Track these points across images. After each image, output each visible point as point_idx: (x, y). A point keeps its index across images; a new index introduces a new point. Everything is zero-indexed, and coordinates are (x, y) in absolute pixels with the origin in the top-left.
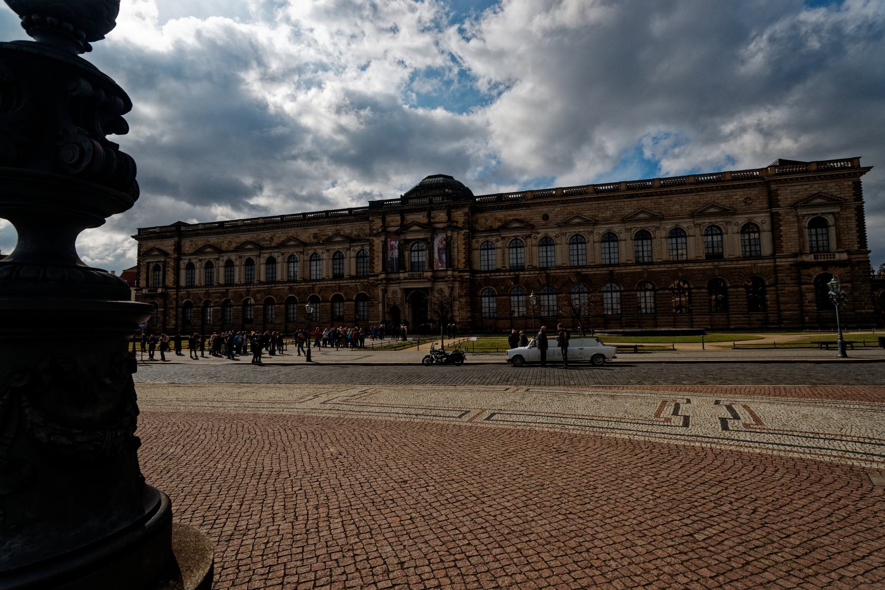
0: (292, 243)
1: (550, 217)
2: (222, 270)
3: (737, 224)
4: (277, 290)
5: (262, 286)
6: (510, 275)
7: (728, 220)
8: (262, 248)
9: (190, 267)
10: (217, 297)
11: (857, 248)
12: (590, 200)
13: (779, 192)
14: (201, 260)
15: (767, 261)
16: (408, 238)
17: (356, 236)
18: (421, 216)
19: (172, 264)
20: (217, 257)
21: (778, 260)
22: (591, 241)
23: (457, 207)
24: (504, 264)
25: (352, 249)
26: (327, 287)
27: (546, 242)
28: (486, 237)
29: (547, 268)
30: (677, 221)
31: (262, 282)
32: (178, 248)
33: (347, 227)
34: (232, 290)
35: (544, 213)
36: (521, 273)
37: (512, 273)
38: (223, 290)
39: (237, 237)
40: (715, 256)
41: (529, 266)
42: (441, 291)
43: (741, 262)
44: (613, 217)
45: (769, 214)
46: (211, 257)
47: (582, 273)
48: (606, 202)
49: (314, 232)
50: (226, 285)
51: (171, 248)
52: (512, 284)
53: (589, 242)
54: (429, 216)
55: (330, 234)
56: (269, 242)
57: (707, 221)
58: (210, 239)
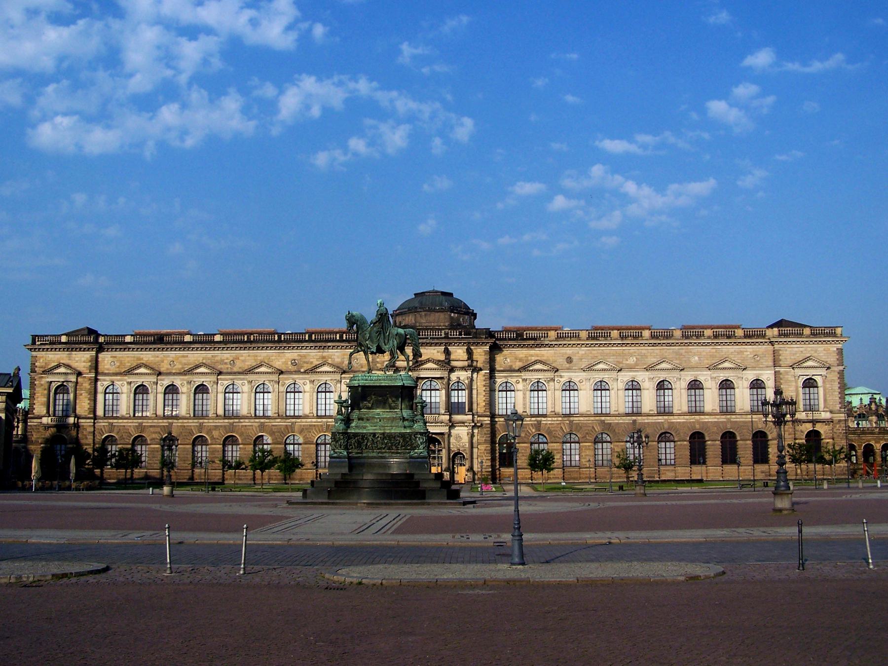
1: (574, 360)
2: (160, 397)
3: (747, 379)
4: (242, 426)
6: (530, 421)
8: (220, 373)
10: (156, 433)
13: (780, 352)
14: (130, 383)
16: (422, 376)
18: (435, 351)
19: (86, 385)
23: (477, 344)
24: (525, 408)
26: (310, 425)
27: (570, 387)
28: (505, 377)
29: (570, 415)
30: (696, 373)
31: (220, 416)
32: (95, 365)
33: (337, 354)
34: (176, 423)
36: (543, 419)
37: (533, 419)
38: (165, 423)
39: (183, 357)
40: (727, 410)
41: (552, 412)
42: (458, 438)
44: (636, 364)
45: (773, 372)
46: (147, 381)
47: (606, 422)
51: (85, 364)
52: (534, 430)
54: (447, 352)
57: (721, 375)
58: (142, 356)
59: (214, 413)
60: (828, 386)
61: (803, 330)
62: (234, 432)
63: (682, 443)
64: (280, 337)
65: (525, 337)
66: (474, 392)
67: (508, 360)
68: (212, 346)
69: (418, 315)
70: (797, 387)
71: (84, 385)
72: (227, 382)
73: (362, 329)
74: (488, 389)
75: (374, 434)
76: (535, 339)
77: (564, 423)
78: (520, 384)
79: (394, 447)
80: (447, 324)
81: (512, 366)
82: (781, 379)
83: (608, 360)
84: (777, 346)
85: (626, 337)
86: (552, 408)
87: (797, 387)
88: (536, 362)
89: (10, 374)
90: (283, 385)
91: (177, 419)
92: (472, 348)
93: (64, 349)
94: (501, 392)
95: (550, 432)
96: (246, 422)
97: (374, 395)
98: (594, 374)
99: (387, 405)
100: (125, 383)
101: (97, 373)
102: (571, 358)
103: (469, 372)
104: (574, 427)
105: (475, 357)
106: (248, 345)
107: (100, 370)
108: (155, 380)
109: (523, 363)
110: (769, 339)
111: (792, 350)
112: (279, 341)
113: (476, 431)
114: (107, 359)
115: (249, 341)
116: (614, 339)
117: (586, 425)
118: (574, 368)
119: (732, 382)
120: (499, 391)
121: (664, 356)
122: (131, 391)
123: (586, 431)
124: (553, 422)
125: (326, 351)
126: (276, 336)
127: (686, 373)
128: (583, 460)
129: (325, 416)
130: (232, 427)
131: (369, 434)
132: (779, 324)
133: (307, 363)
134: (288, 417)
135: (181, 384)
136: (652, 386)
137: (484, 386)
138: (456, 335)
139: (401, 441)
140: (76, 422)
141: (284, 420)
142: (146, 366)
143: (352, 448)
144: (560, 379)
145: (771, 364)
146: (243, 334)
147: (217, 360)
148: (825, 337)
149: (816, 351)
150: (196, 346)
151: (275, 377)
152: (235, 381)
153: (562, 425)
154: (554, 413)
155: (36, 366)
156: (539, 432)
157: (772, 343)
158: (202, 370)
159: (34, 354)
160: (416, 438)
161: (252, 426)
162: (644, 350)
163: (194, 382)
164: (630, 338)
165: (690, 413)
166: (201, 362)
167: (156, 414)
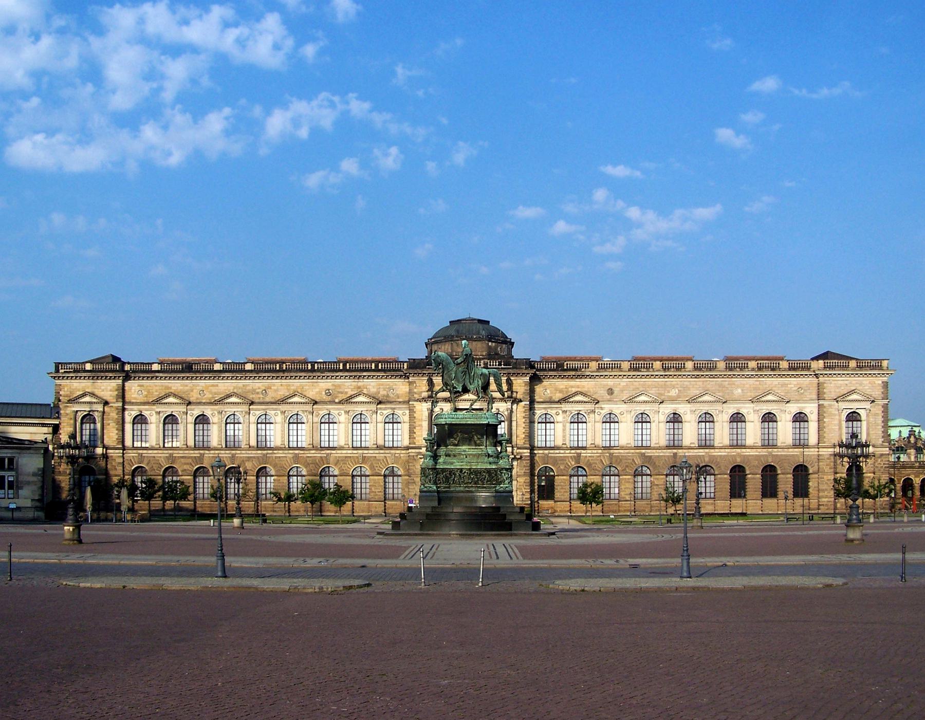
1: (615, 392)
2: (191, 427)
5: (254, 452)
6: (570, 453)
8: (252, 403)
9: (140, 420)
10: (188, 464)
11: (881, 442)
13: (825, 385)
14: (159, 413)
15: (812, 450)
16: (460, 407)
17: (384, 396)
19: (113, 414)
21: (821, 449)
22: (657, 421)
24: (564, 440)
25: (379, 412)
26: (346, 457)
27: (610, 419)
28: (545, 408)
29: (610, 448)
30: (739, 405)
31: (253, 447)
32: (122, 395)
35: (609, 388)
36: (583, 451)
37: (573, 451)
38: (196, 453)
39: (213, 386)
40: (768, 444)
41: (591, 444)
43: (791, 450)
44: (678, 396)
45: (817, 405)
46: (177, 410)
47: (646, 454)
50: (196, 448)
52: (573, 463)
53: (654, 421)
55: (350, 393)
57: (764, 408)
58: (170, 385)
59: (246, 445)
60: (871, 419)
61: (848, 363)
62: (268, 464)
63: (722, 476)
64: (313, 366)
65: (565, 368)
66: (514, 424)
67: (548, 391)
68: (243, 374)
69: (454, 344)
70: (840, 421)
71: (111, 414)
72: (260, 412)
73: (448, 369)
74: (528, 421)
75: (461, 470)
76: (575, 370)
77: (604, 456)
78: (560, 416)
79: (480, 482)
80: (484, 354)
81: (552, 397)
82: (825, 412)
83: (650, 392)
84: (821, 379)
85: (668, 369)
86: (592, 440)
87: (840, 421)
88: (576, 394)
89: (50, 405)
90: (317, 416)
91: (208, 450)
92: (512, 378)
93: (89, 377)
94: (540, 424)
95: (589, 465)
96: (280, 454)
97: (460, 432)
98: (634, 406)
99: (473, 442)
100: (154, 412)
101: (124, 403)
102: (612, 389)
103: (509, 404)
104: (614, 460)
105: (514, 388)
106: (281, 374)
107: (127, 399)
108: (185, 410)
109: (563, 394)
110: (814, 371)
111: (836, 383)
112: (313, 370)
113: (515, 463)
114: (133, 388)
115: (281, 370)
116: (657, 371)
117: (626, 458)
118: (615, 400)
119: (775, 415)
120: (539, 423)
121: (706, 389)
122: (160, 421)
123: (627, 464)
124: (592, 455)
125: (361, 380)
126: (309, 365)
127: (728, 405)
128: (622, 493)
129: (361, 447)
130: (265, 459)
131: (456, 470)
132: (825, 356)
133: (342, 393)
134: (322, 448)
135: (212, 414)
136: (694, 418)
137: (524, 417)
138: (496, 365)
139: (487, 476)
140: (104, 452)
141: (319, 452)
142: (175, 396)
143: (441, 483)
144: (601, 411)
145: (815, 397)
146: (275, 362)
147: (249, 390)
148: (871, 370)
149: (861, 384)
150: (227, 375)
151: (309, 408)
152: (268, 411)
153: (602, 458)
154: (593, 446)
155: (61, 395)
156: (579, 465)
157: (817, 376)
158: (233, 399)
159: (58, 382)
160: (502, 473)
161: (286, 457)
162: (687, 382)
163: (225, 412)
164: (673, 370)
165: (732, 446)
166: (232, 391)
167: (187, 445)
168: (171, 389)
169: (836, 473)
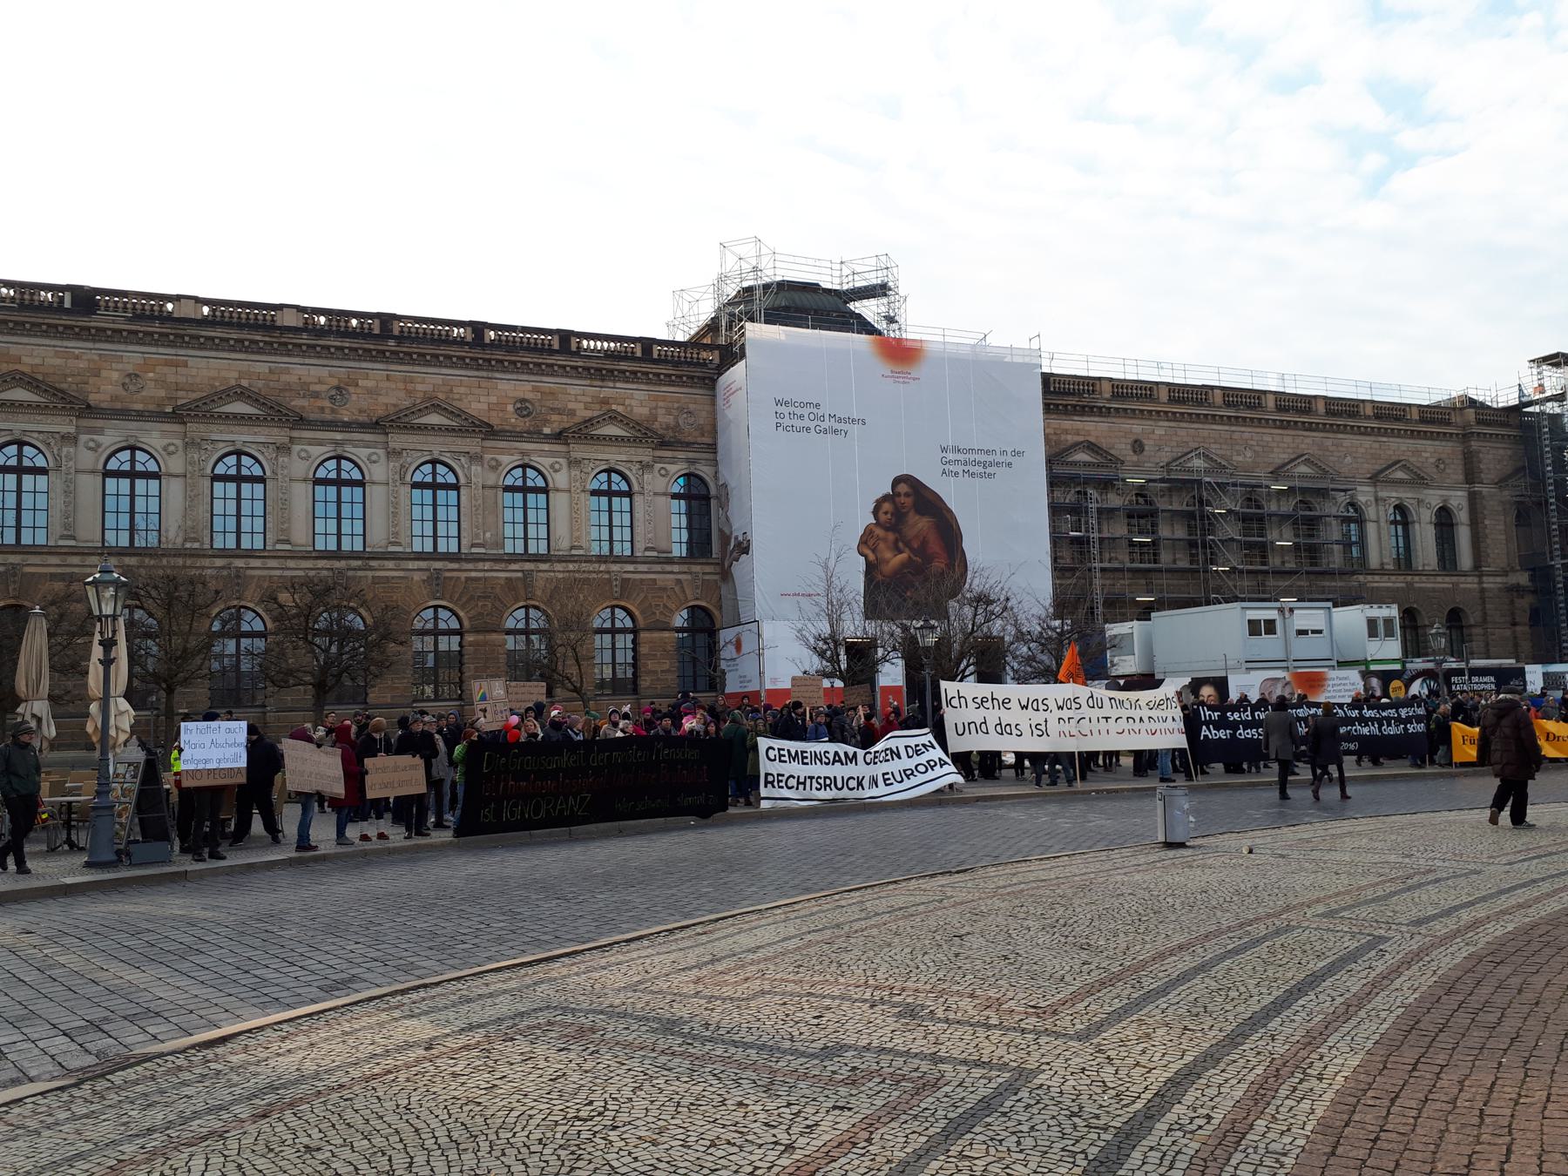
0: (434, 419)
1: (1146, 448)
7: (1421, 497)
8: (301, 421)
12: (1214, 419)
17: (668, 428)
20: (72, 429)
21: (1485, 579)
35: (1135, 437)
39: (168, 364)
43: (1439, 579)
45: (1465, 494)
48: (1243, 429)
49: (520, 395)
56: (327, 404)
57: (1394, 494)
58: (14, 350)
72: (324, 449)
84: (1475, 445)
96: (389, 570)
102: (1141, 442)
121: (1300, 452)
125: (611, 384)
133: (559, 412)
157: (1466, 437)
161: (406, 578)
166: (233, 383)
168: (19, 360)
169: (1514, 624)
